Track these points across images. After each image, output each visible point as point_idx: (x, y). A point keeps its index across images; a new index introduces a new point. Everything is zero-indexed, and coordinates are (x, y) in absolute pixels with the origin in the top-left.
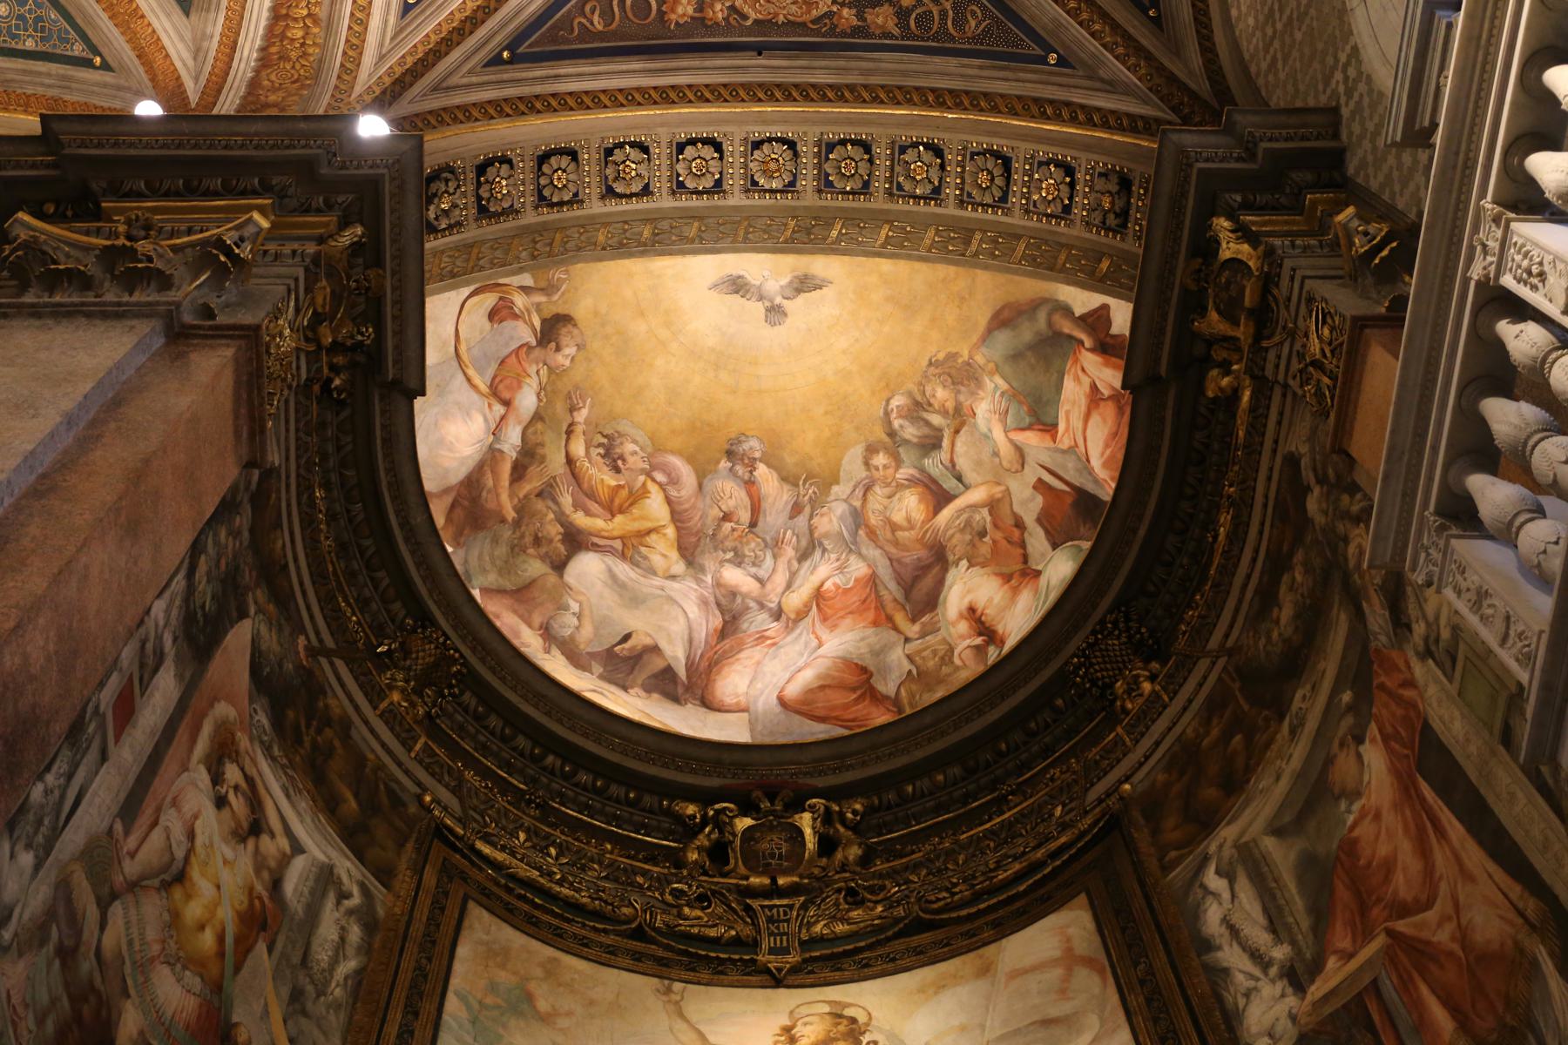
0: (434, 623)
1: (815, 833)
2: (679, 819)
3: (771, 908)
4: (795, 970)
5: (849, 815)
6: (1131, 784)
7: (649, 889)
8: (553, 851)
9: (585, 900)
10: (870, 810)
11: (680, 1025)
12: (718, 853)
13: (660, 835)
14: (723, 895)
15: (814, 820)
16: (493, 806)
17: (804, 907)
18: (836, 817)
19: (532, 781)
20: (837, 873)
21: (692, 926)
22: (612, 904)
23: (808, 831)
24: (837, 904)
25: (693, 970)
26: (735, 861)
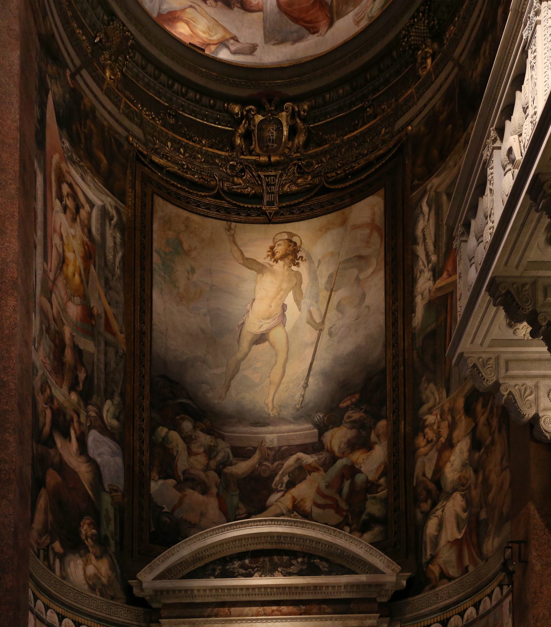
0: (117, 17)
1: (287, 124)
2: (232, 114)
3: (268, 176)
4: (276, 213)
5: (302, 113)
6: (412, 126)
7: (221, 166)
8: (182, 150)
9: (196, 180)
10: (311, 108)
11: (235, 248)
12: (247, 136)
13: (224, 124)
14: (249, 166)
15: (287, 116)
16: (156, 130)
17: (281, 176)
18: (296, 114)
19: (169, 100)
20: (295, 153)
21: (238, 189)
22: (207, 181)
23: (284, 124)
24: (294, 173)
25: (239, 214)
26: (255, 146)
